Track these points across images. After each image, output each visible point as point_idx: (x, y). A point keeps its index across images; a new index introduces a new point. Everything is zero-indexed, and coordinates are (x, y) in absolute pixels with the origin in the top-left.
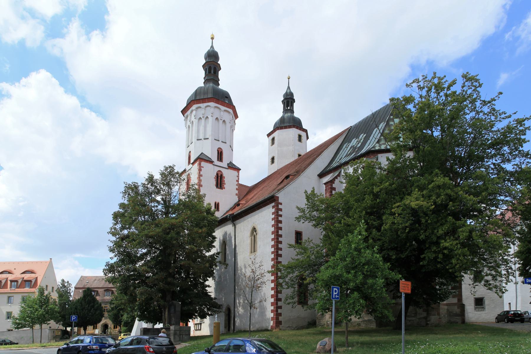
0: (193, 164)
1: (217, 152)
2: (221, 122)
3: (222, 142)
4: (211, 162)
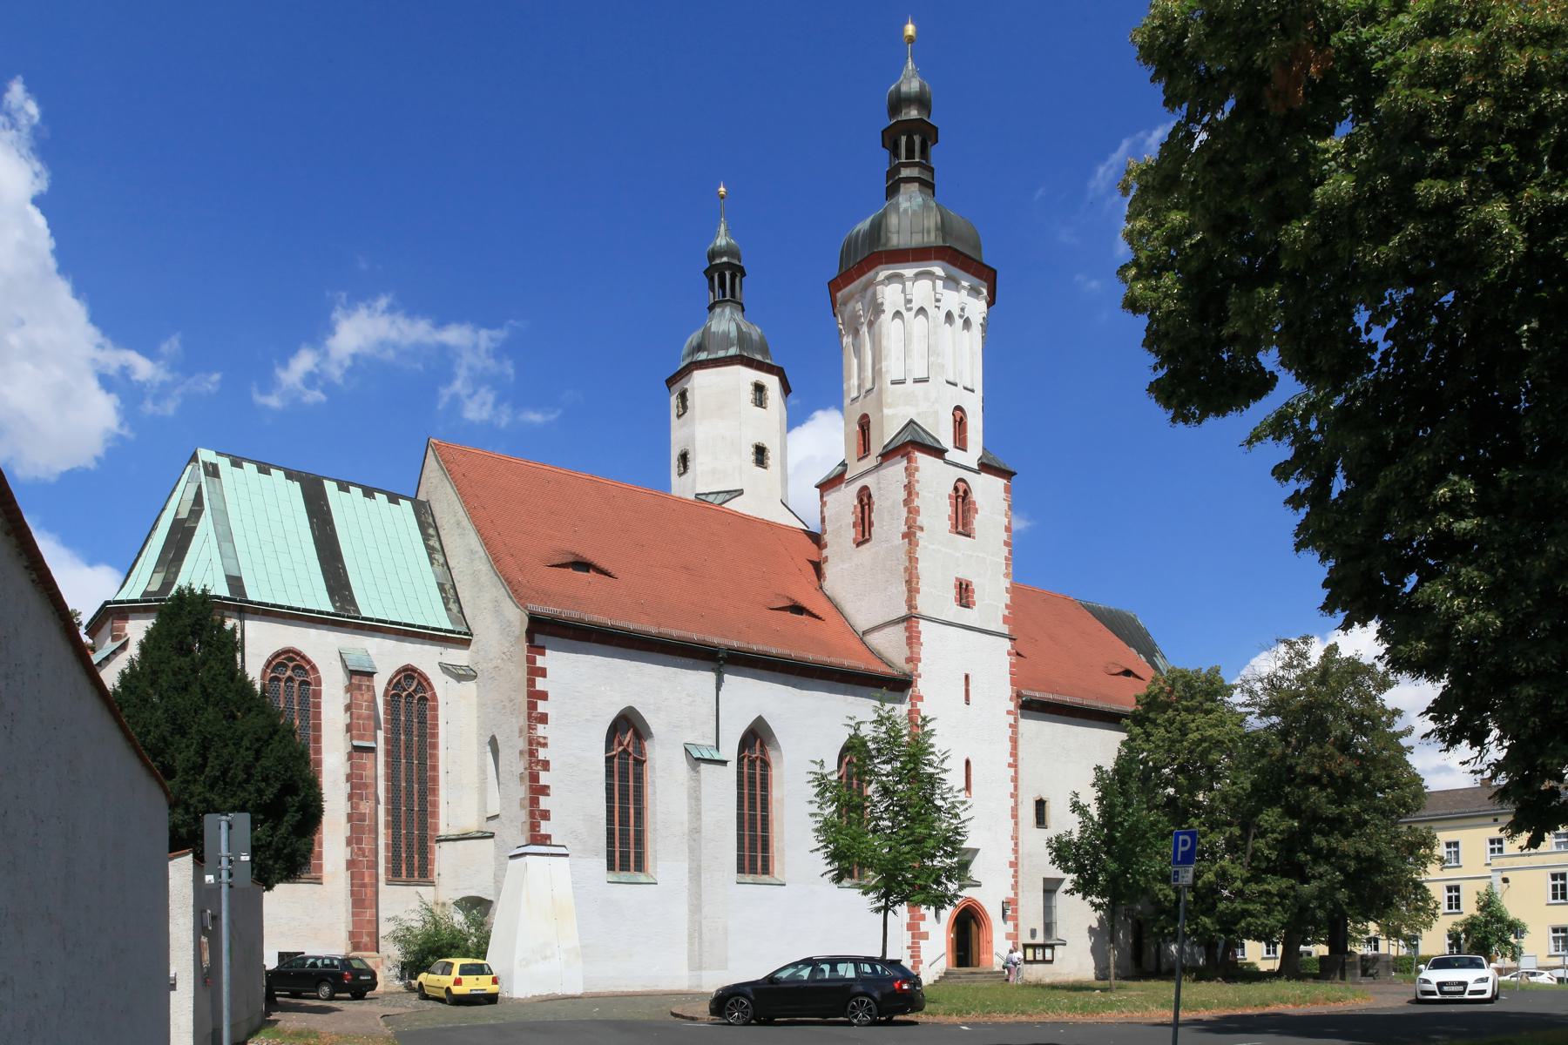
0: (888, 455)
1: (952, 417)
2: (959, 322)
3: (965, 388)
4: (939, 452)
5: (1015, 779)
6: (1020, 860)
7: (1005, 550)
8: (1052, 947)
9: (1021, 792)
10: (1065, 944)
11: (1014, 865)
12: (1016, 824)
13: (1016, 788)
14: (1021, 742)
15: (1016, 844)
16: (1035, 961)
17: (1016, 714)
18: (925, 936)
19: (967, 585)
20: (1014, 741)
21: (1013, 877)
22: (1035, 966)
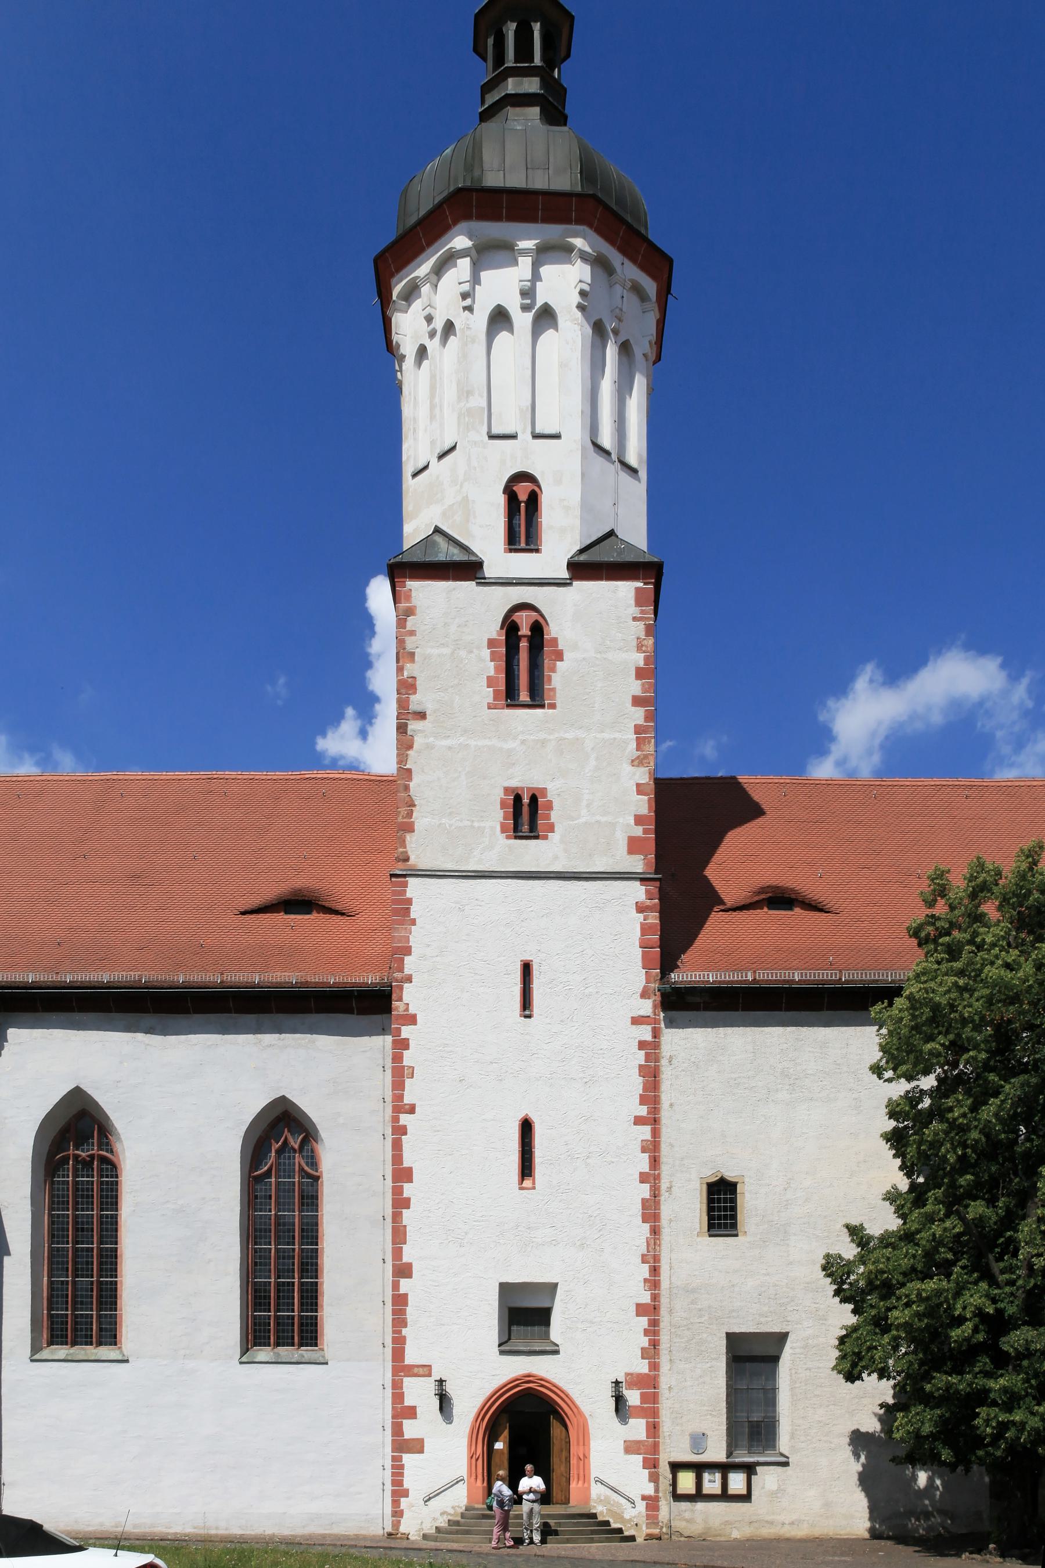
5: (653, 1149)
6: (664, 1301)
7: (638, 715)
8: (749, 1469)
9: (665, 1170)
10: (786, 1464)
11: (650, 1311)
12: (655, 1231)
13: (655, 1162)
14: (667, 1074)
15: (655, 1270)
16: (699, 1496)
17: (656, 1021)
18: (417, 1446)
19: (534, 799)
20: (651, 1074)
21: (646, 1332)
22: (700, 1506)
